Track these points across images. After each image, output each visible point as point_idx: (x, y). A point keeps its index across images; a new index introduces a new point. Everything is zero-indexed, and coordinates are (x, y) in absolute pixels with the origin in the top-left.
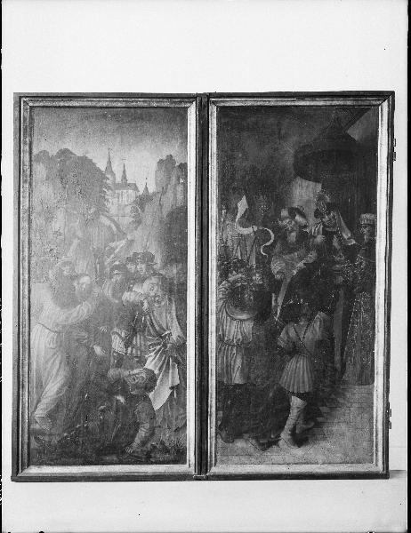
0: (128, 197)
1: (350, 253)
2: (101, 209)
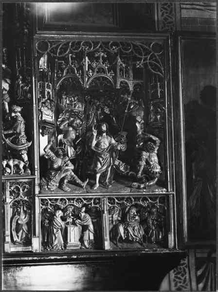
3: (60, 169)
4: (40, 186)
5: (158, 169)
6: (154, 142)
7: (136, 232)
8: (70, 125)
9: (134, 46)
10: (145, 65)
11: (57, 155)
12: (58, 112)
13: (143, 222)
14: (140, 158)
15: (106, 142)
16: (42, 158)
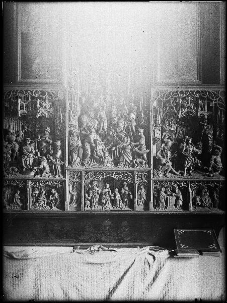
3: (164, 164)
4: (154, 174)
6: (219, 149)
7: (207, 200)
8: (169, 138)
9: (209, 92)
10: (215, 104)
11: (163, 157)
12: (163, 131)
13: (211, 196)
14: (210, 159)
15: (192, 148)
16: (154, 157)
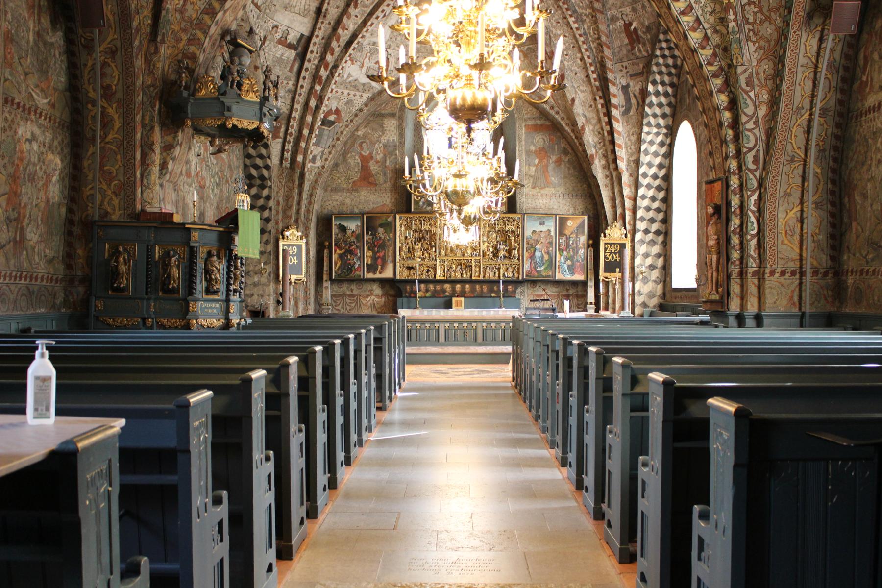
0: (351, 232)
1: (388, 240)
2: (346, 233)
5: (517, 256)
15: (502, 247)
